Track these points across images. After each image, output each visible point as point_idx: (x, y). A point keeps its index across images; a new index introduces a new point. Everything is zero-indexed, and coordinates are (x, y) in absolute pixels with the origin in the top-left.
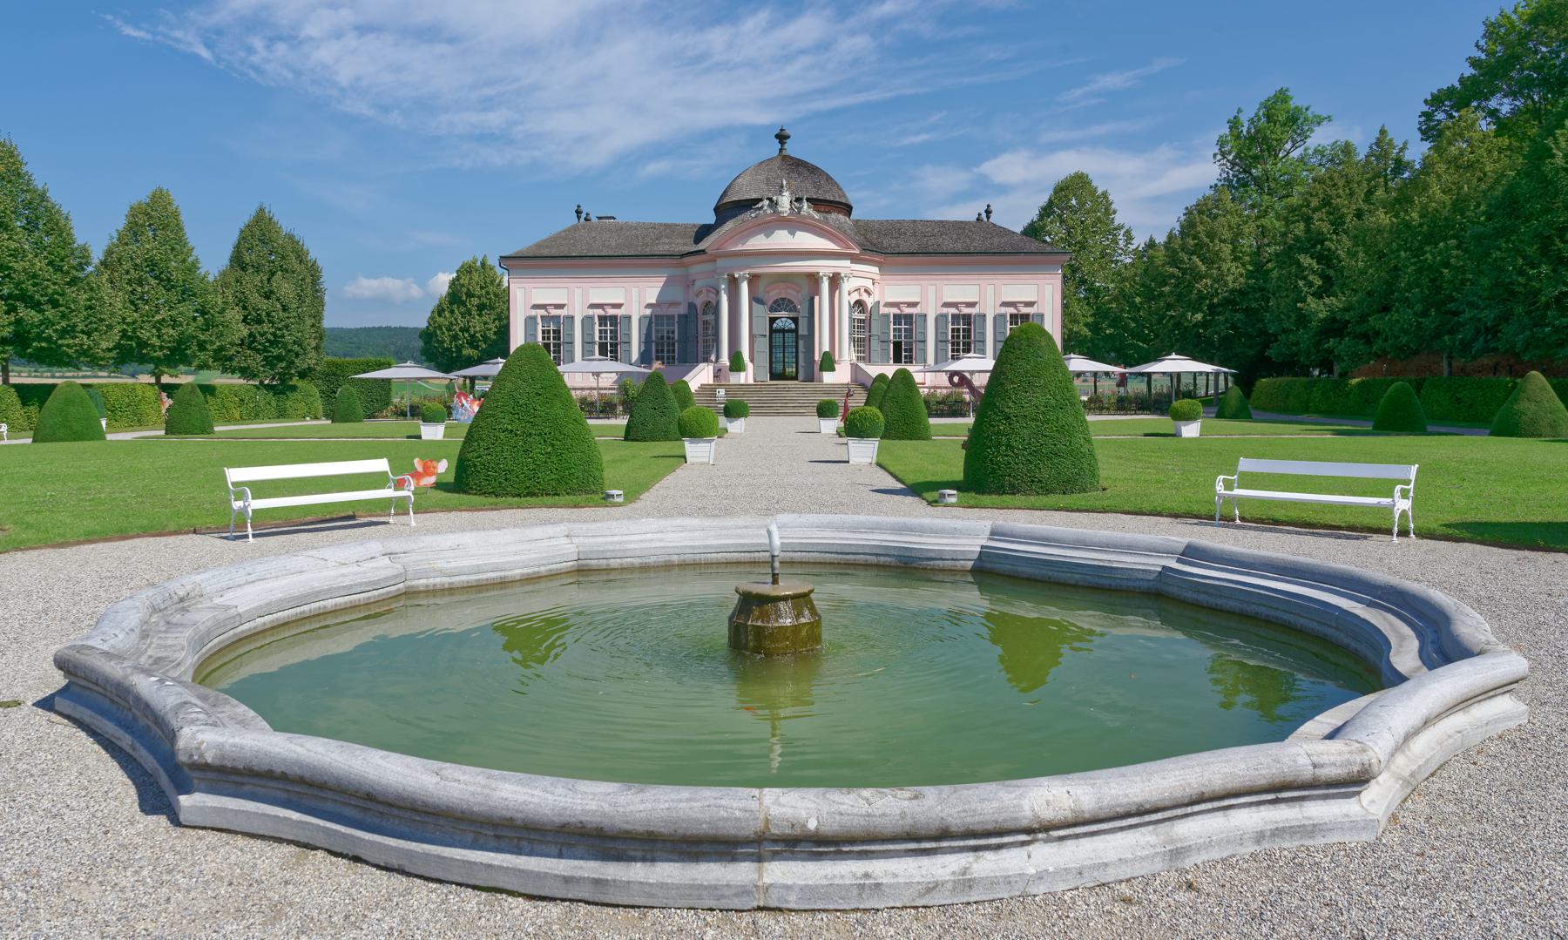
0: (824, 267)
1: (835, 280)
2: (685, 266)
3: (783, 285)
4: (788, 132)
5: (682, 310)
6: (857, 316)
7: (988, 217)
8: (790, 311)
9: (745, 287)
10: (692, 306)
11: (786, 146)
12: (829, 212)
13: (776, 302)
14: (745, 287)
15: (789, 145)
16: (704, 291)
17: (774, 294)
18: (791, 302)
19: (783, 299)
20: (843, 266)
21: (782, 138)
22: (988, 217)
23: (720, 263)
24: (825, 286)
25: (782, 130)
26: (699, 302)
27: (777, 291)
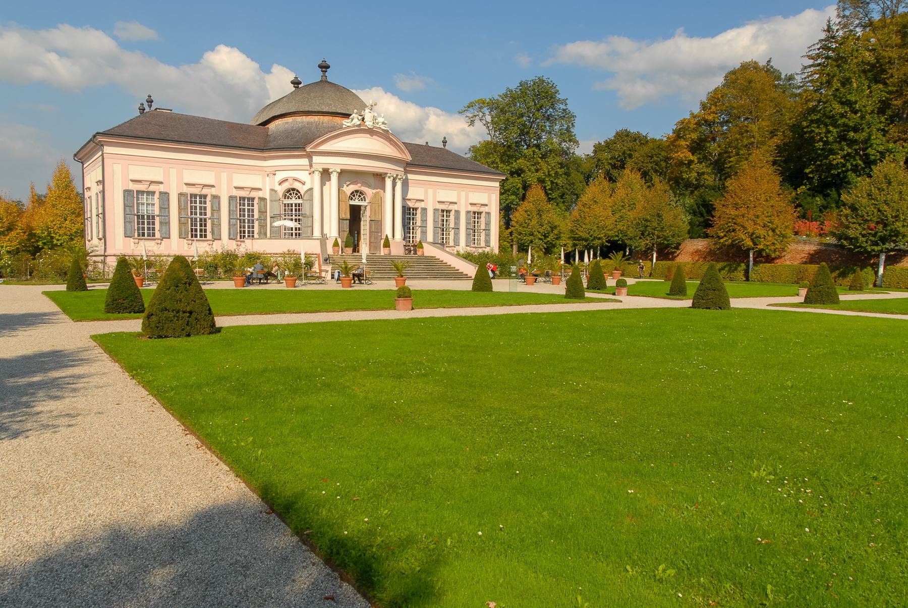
16: (290, 181)
17: (353, 188)
23: (316, 159)
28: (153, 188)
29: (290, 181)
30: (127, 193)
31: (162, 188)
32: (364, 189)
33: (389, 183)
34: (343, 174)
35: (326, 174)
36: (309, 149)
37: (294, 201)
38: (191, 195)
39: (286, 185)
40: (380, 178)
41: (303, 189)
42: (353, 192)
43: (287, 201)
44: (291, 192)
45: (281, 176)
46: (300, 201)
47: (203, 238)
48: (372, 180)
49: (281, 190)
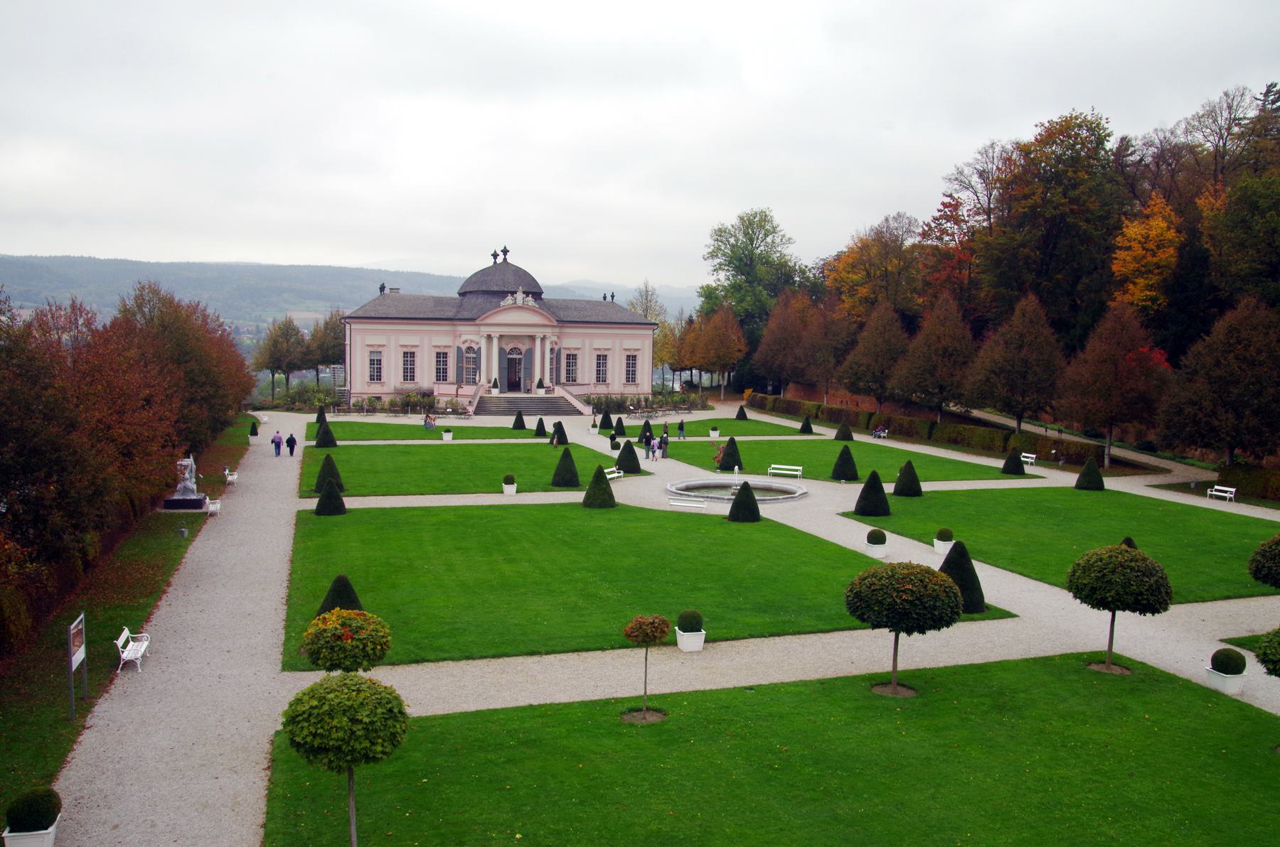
0: (539, 332)
1: (543, 339)
2: (455, 325)
3: (516, 342)
4: (508, 248)
7: (613, 299)
8: (519, 354)
9: (495, 342)
11: (507, 257)
14: (495, 342)
16: (469, 342)
17: (511, 346)
20: (548, 331)
23: (483, 329)
25: (505, 248)
26: (464, 347)
27: (512, 344)
32: (520, 346)
33: (538, 342)
34: (501, 337)
35: (489, 337)
36: (477, 322)
37: (472, 355)
39: (467, 345)
40: (532, 338)
41: (476, 348)
43: (468, 355)
44: (470, 349)
45: (464, 337)
46: (474, 355)
47: (409, 382)
49: (464, 347)
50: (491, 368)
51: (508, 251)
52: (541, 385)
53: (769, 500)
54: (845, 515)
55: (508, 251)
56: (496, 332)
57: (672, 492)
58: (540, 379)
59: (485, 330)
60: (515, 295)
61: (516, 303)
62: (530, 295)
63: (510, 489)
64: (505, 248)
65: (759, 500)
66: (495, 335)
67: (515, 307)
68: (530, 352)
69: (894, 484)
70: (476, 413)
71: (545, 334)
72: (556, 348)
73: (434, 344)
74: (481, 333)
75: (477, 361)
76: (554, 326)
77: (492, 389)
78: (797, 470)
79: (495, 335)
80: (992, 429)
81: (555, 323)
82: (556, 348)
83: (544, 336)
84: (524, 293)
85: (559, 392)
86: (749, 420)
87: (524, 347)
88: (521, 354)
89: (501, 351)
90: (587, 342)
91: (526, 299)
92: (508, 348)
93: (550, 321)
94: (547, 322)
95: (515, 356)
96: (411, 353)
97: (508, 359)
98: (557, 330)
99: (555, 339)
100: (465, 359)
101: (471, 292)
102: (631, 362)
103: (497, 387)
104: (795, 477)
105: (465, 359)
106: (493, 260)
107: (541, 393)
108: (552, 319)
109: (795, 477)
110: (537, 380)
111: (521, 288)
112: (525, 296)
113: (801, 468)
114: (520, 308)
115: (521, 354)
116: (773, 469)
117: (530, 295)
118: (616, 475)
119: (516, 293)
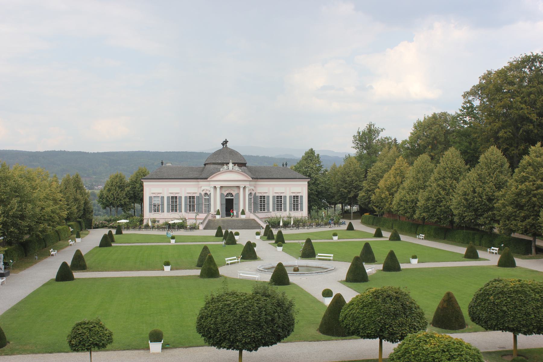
0: (242, 185)
1: (244, 188)
2: (198, 181)
4: (228, 140)
5: (198, 195)
6: (250, 197)
7: (286, 166)
9: (218, 190)
10: (200, 194)
12: (241, 167)
13: (227, 194)
14: (218, 190)
15: (228, 145)
16: (205, 190)
17: (227, 192)
18: (232, 194)
19: (229, 193)
20: (247, 184)
21: (226, 142)
22: (286, 166)
24: (242, 189)
25: (226, 140)
28: (158, 195)
29: (205, 190)
30: (151, 198)
31: (162, 195)
32: (232, 192)
33: (242, 189)
34: (221, 187)
35: (215, 187)
36: (208, 180)
37: (207, 197)
38: (172, 197)
39: (204, 192)
40: (238, 187)
42: (228, 194)
44: (206, 194)
45: (203, 188)
46: (208, 198)
48: (236, 189)
49: (203, 193)
50: (217, 204)
51: (228, 142)
52: (243, 213)
53: (306, 273)
54: (341, 282)
55: (228, 142)
56: (218, 185)
57: (259, 270)
58: (243, 210)
59: (213, 184)
60: (228, 165)
61: (228, 169)
62: (236, 165)
63: (167, 268)
64: (226, 140)
65: (289, 273)
66: (218, 187)
67: (228, 171)
68: (238, 195)
69: (383, 265)
70: (205, 229)
71: (245, 185)
72: (253, 193)
73: (187, 192)
74: (211, 186)
75: (209, 200)
76: (251, 181)
77: (216, 216)
78: (330, 257)
79: (218, 187)
80: (468, 231)
81: (251, 179)
82: (253, 193)
83: (245, 186)
84: (233, 163)
85: (252, 216)
86: (355, 230)
87: (234, 193)
88: (233, 196)
89: (222, 195)
90: (271, 188)
91: (234, 167)
92: (225, 194)
93: (248, 178)
94: (246, 179)
95: (229, 198)
96: (175, 197)
97: (226, 199)
98: (253, 183)
99: (253, 188)
100: (203, 200)
101: (207, 164)
102: (296, 199)
103: (219, 215)
104: (330, 260)
105: (203, 200)
106: (222, 146)
107: (243, 217)
108: (249, 177)
109: (330, 260)
110: (241, 211)
111: (231, 161)
112: (233, 165)
113: (332, 255)
114: (231, 171)
115: (233, 196)
116: (319, 256)
117: (236, 165)
118: (236, 261)
119: (228, 163)
